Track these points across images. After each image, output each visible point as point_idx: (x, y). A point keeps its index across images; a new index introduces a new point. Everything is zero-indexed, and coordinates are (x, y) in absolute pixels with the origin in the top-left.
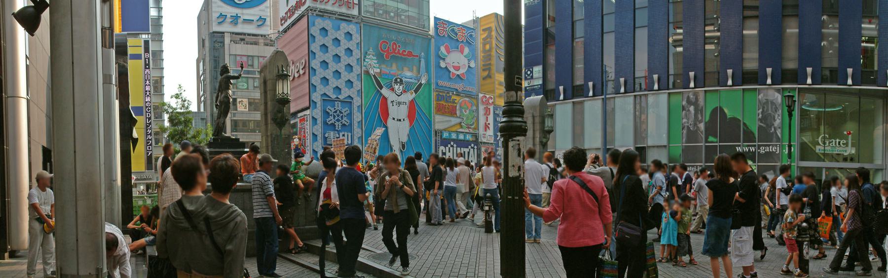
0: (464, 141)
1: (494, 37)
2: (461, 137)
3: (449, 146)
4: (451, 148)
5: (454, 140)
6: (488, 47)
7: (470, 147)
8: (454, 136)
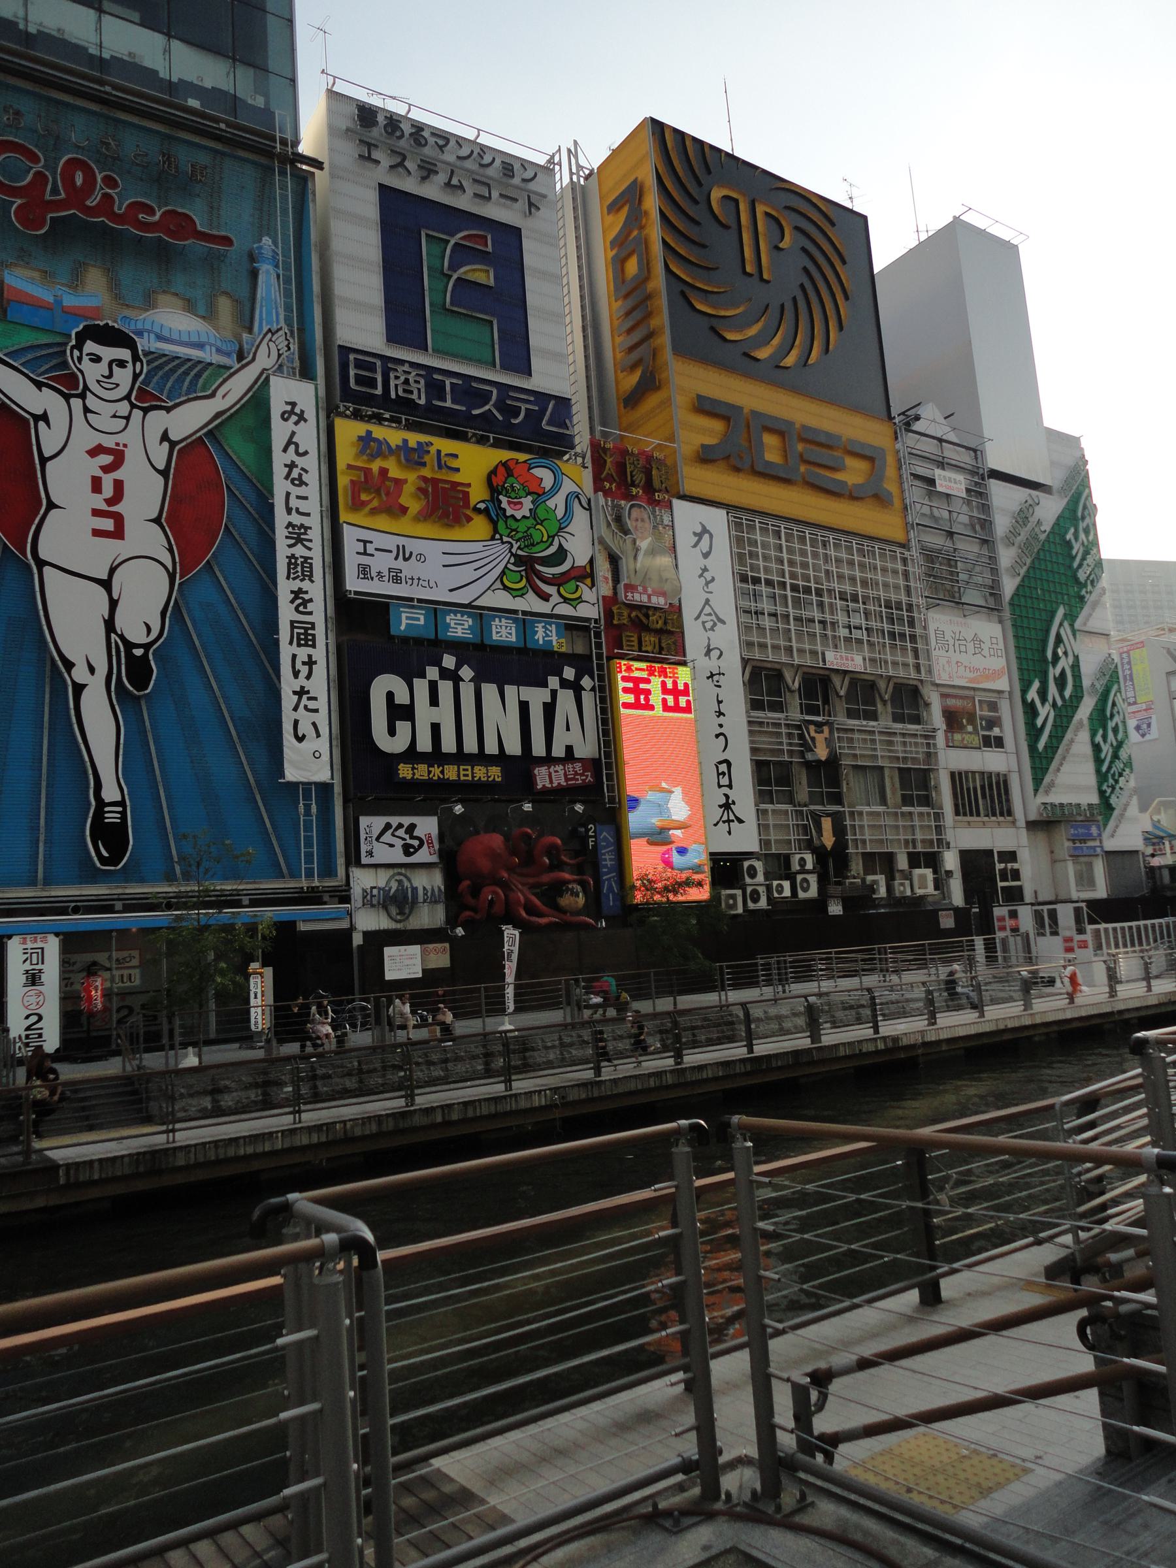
1: (655, 215)
2: (503, 633)
3: (432, 673)
4: (445, 688)
5: (456, 647)
6: (632, 267)
7: (554, 682)
8: (459, 628)
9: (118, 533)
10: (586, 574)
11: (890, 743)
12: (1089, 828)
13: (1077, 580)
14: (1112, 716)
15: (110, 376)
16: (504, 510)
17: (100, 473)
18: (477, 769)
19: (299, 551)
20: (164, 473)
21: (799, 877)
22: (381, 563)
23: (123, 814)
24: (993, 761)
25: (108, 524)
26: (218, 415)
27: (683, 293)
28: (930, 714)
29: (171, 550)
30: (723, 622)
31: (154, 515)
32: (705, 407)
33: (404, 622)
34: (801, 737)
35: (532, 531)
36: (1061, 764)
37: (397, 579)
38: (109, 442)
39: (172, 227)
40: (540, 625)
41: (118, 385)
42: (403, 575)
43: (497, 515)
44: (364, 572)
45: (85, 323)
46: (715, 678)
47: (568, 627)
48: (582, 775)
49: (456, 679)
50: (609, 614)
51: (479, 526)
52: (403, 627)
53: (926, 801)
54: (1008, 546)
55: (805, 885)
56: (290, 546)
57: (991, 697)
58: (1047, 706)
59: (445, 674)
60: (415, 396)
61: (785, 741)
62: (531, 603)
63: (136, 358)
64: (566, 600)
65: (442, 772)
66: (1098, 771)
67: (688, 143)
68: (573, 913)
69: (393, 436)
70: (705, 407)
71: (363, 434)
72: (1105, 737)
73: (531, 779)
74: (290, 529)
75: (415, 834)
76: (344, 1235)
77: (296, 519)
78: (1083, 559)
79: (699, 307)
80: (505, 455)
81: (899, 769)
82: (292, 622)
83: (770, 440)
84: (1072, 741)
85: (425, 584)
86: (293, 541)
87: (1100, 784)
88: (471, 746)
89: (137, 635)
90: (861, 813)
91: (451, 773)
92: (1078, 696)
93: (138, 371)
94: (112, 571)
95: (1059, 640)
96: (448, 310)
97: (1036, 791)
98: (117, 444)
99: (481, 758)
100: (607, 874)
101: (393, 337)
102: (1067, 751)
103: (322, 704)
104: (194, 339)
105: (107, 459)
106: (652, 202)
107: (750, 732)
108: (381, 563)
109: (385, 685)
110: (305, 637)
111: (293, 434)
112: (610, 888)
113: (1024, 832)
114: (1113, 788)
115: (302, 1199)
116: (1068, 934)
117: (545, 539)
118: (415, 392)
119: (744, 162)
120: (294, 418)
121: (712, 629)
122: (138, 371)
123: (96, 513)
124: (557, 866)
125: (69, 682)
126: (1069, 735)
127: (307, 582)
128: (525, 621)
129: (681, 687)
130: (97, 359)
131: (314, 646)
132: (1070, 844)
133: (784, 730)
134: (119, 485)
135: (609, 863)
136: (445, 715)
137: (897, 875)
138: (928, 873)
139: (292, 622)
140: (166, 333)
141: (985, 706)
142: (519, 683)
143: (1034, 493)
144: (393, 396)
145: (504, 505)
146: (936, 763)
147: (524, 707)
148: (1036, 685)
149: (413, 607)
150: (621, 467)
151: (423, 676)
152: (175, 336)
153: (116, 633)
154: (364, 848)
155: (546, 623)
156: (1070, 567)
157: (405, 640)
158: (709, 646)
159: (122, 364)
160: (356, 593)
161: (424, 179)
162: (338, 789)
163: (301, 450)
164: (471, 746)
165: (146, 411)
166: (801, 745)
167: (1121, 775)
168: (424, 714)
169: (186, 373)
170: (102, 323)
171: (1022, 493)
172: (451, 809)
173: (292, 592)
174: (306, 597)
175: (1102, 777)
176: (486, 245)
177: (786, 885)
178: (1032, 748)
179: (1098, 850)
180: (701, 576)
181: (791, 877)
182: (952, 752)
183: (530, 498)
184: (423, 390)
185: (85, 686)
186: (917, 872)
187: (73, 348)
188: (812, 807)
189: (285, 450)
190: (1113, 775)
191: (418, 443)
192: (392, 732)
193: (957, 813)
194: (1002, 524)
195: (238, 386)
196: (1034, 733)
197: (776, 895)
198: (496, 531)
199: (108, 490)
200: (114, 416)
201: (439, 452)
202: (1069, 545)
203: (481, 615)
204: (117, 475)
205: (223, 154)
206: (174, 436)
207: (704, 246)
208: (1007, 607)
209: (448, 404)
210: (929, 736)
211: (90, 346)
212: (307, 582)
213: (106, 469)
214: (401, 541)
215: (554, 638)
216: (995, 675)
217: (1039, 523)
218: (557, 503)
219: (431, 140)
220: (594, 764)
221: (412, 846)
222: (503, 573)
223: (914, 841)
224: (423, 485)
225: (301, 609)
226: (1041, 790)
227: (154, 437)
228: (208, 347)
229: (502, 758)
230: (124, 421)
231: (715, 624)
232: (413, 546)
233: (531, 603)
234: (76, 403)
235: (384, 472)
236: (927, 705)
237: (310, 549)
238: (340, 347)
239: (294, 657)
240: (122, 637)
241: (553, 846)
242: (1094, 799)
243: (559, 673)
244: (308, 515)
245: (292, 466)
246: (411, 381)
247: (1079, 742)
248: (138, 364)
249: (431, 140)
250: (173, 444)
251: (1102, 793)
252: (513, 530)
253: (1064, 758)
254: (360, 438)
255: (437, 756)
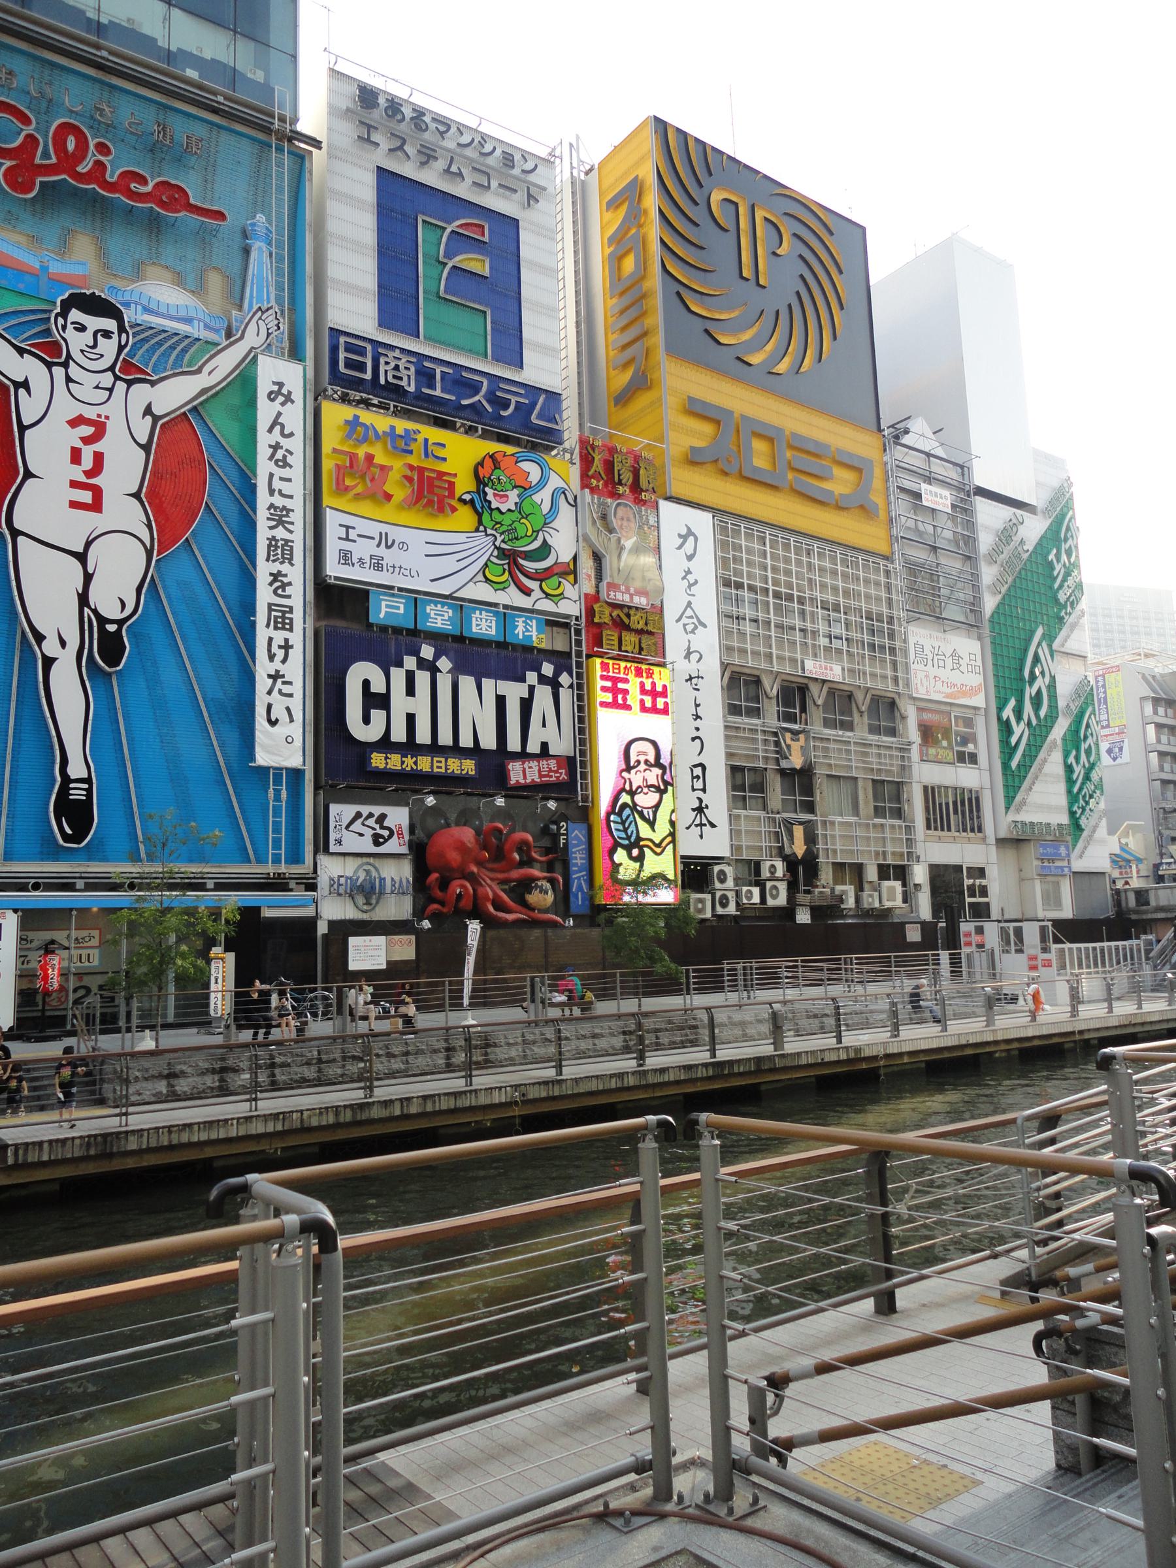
0: (502, 645)
1: (654, 214)
2: (483, 626)
3: (410, 662)
4: (422, 679)
5: (437, 638)
6: (629, 264)
7: (531, 677)
8: (439, 619)
9: (96, 506)
10: (570, 571)
11: (866, 754)
12: (1057, 848)
13: (1057, 601)
14: (1086, 738)
15: (95, 346)
16: (490, 502)
17: (79, 444)
18: (450, 761)
19: (280, 533)
20: (146, 448)
21: (769, 884)
22: (363, 549)
23: (89, 791)
24: (967, 777)
25: (86, 497)
26: (204, 391)
27: (678, 293)
28: (906, 728)
29: (149, 526)
30: (705, 626)
31: (134, 490)
32: (696, 409)
33: (384, 609)
34: (777, 744)
35: (516, 524)
36: (1033, 783)
37: (378, 566)
38: (90, 413)
39: (164, 198)
40: (520, 620)
41: (102, 356)
42: (384, 563)
43: (482, 507)
44: (345, 558)
45: (71, 291)
46: (694, 681)
47: (551, 624)
48: (556, 772)
49: (434, 670)
50: (590, 613)
51: (465, 517)
52: (382, 615)
53: (898, 813)
54: (990, 564)
55: (774, 892)
56: (271, 528)
57: (968, 714)
58: (1022, 725)
59: (422, 664)
60: (404, 383)
61: (761, 747)
62: (512, 597)
63: (122, 329)
64: (547, 595)
65: (416, 763)
66: (1069, 792)
67: (691, 144)
68: (541, 911)
69: (380, 421)
70: (696, 409)
71: (350, 418)
72: (1077, 758)
73: (503, 775)
74: (272, 511)
75: (385, 824)
76: (304, 1216)
77: (279, 501)
78: (1064, 580)
79: (694, 308)
80: (494, 447)
81: (873, 780)
82: (270, 605)
83: (759, 446)
84: (1045, 761)
85: (407, 573)
86: (274, 523)
87: (1071, 804)
88: (445, 738)
89: (111, 611)
90: (832, 823)
91: (424, 764)
92: (1052, 717)
93: (123, 343)
94: (88, 544)
95: (1036, 659)
96: (440, 298)
97: (1007, 809)
98: (99, 416)
99: (456, 750)
100: (577, 872)
101: (385, 321)
102: (1040, 770)
103: (297, 689)
104: (182, 313)
105: (88, 431)
106: (652, 201)
107: (727, 737)
108: (363, 549)
109: (361, 673)
110: (282, 621)
111: (279, 414)
112: (580, 888)
113: (993, 849)
114: (1084, 809)
115: (262, 1180)
116: (1032, 952)
117: (529, 533)
118: (405, 379)
119: (746, 166)
120: (281, 399)
121: (693, 632)
122: (123, 343)
123: (74, 484)
124: (528, 862)
125: (39, 655)
126: (1041, 755)
127: (287, 565)
128: (506, 615)
129: (659, 688)
130: (81, 328)
131: (291, 630)
132: (1039, 863)
133: (760, 737)
134: (99, 458)
135: (579, 862)
136: (420, 705)
137: (866, 886)
138: (897, 885)
139: (270, 605)
140: (153, 306)
141: (961, 722)
142: (497, 677)
143: (1019, 512)
144: (382, 382)
145: (490, 497)
146: (910, 777)
147: (501, 701)
148: (1012, 703)
149: (393, 595)
150: (609, 465)
151: (400, 664)
152: (163, 310)
153: (89, 607)
154: (333, 836)
155: (527, 618)
156: (1051, 588)
157: (384, 629)
158: (689, 648)
159: (107, 334)
160: (336, 578)
161: (423, 164)
162: (309, 776)
163: (287, 432)
164: (445, 738)
165: (130, 383)
166: (777, 752)
167: (1091, 797)
168: (400, 703)
169: (172, 348)
170: (88, 292)
171: (1007, 512)
172: (422, 801)
173: (271, 574)
174: (285, 580)
175: (1073, 798)
176: (483, 235)
177: (756, 891)
178: (1006, 766)
179: (1066, 870)
180: (684, 578)
181: (760, 884)
182: (926, 766)
183: (516, 492)
184: (413, 377)
185: (55, 659)
186: (886, 884)
187: (57, 315)
188: (785, 815)
189: (270, 430)
190: (1084, 797)
191: (406, 430)
192: (366, 720)
193: (928, 827)
194: (985, 541)
195: (226, 362)
196: (1008, 751)
197: (745, 901)
198: (480, 522)
199: (87, 462)
200: (97, 387)
201: (426, 440)
202: (1051, 566)
203: (461, 606)
204: (98, 447)
205: (219, 127)
206: (157, 411)
207: (702, 248)
208: (987, 625)
209: (438, 392)
210: (905, 749)
211: (75, 315)
212: (287, 565)
213: (87, 441)
214: (384, 528)
215: (534, 634)
216: (973, 691)
217: (1022, 542)
218: (543, 497)
219: (432, 126)
220: (570, 762)
221: (382, 837)
222: (486, 565)
223: (884, 853)
224: (409, 473)
225: (280, 591)
226: (1012, 808)
227: (137, 409)
228: (196, 322)
229: (476, 751)
230: (108, 393)
231: (696, 627)
232: (396, 534)
233: (512, 597)
234: (58, 372)
235: (370, 458)
236: (904, 718)
237: (291, 532)
238: (331, 329)
239: (270, 640)
240: (95, 611)
241: (525, 842)
242: (1064, 819)
243: (537, 669)
244: (291, 497)
245: (276, 447)
246: (401, 367)
247: (1052, 762)
248: (124, 336)
249: (432, 126)
250: (156, 419)
251: (1072, 814)
252: (497, 523)
253: (1037, 777)
254: (347, 422)
255: (411, 747)
